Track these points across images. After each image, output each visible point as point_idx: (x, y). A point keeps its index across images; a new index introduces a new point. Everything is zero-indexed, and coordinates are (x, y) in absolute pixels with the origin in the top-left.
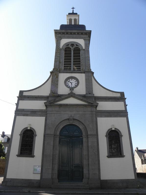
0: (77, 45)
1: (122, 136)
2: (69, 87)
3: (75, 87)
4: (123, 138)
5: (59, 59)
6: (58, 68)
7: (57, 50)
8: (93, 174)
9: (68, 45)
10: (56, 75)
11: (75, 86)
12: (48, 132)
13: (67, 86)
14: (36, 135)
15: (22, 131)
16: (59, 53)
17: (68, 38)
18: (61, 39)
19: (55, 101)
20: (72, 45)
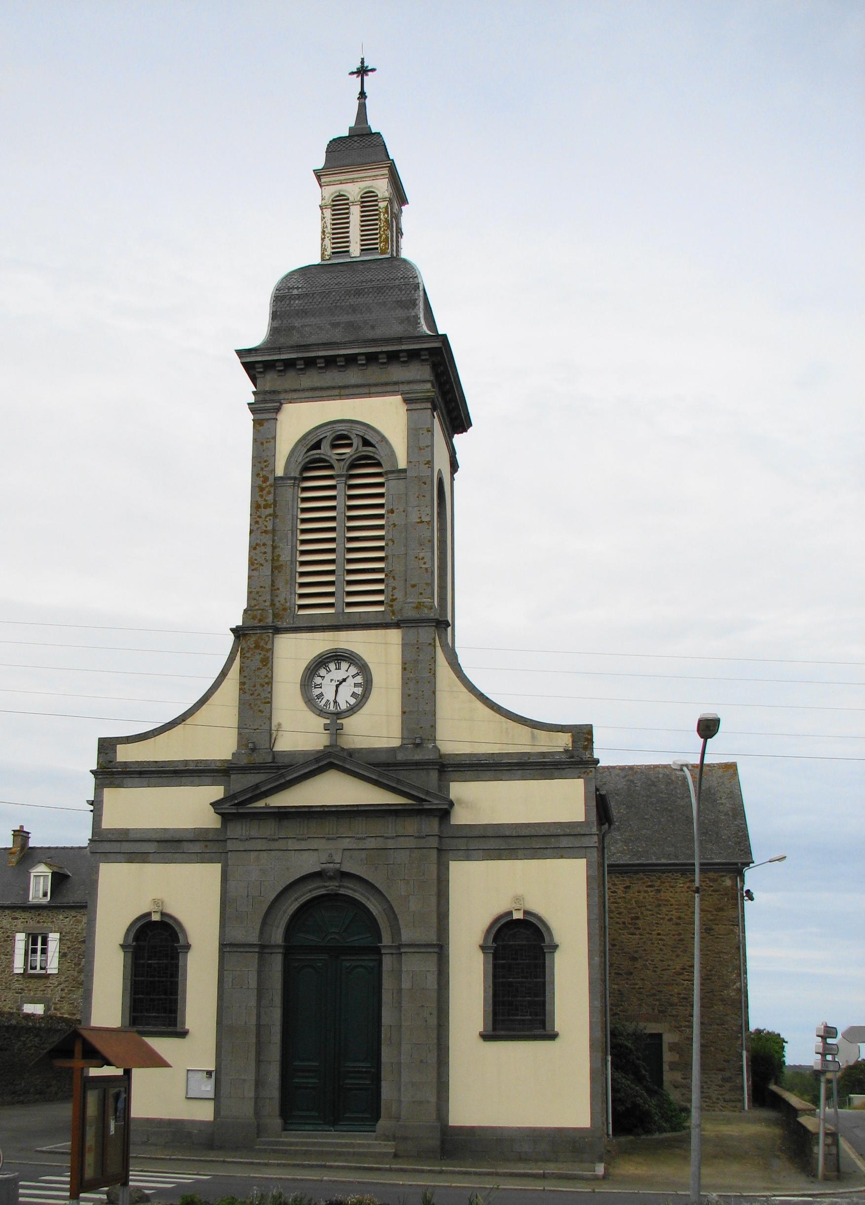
0: (366, 443)
1: (556, 947)
2: (321, 712)
3: (352, 710)
4: (557, 955)
5: (274, 548)
6: (268, 604)
7: (261, 489)
8: (414, 1102)
9: (317, 446)
10: (257, 647)
11: (353, 701)
12: (239, 935)
13: (311, 702)
14: (188, 947)
15: (128, 930)
16: (270, 511)
17: (318, 393)
18: (278, 410)
19: (258, 792)
20: (341, 440)
